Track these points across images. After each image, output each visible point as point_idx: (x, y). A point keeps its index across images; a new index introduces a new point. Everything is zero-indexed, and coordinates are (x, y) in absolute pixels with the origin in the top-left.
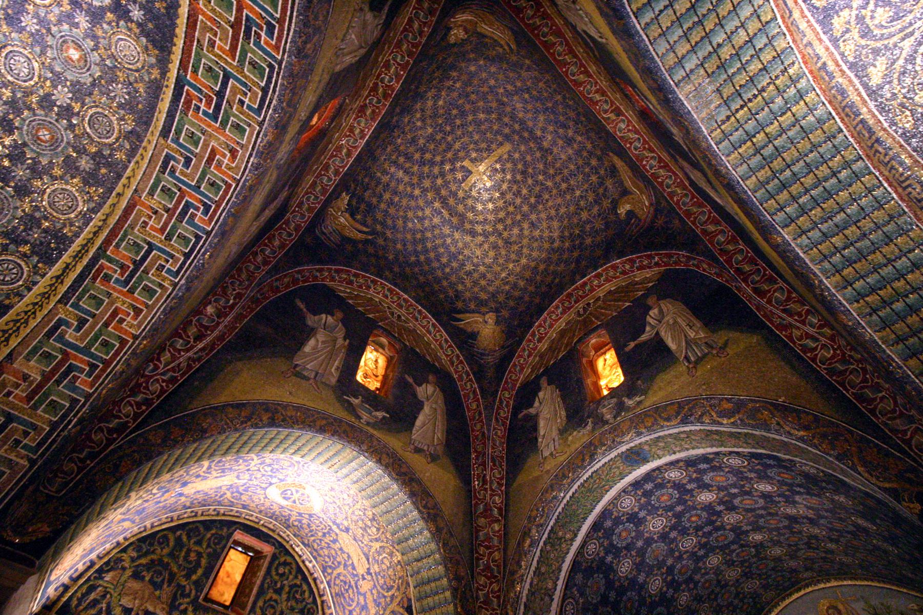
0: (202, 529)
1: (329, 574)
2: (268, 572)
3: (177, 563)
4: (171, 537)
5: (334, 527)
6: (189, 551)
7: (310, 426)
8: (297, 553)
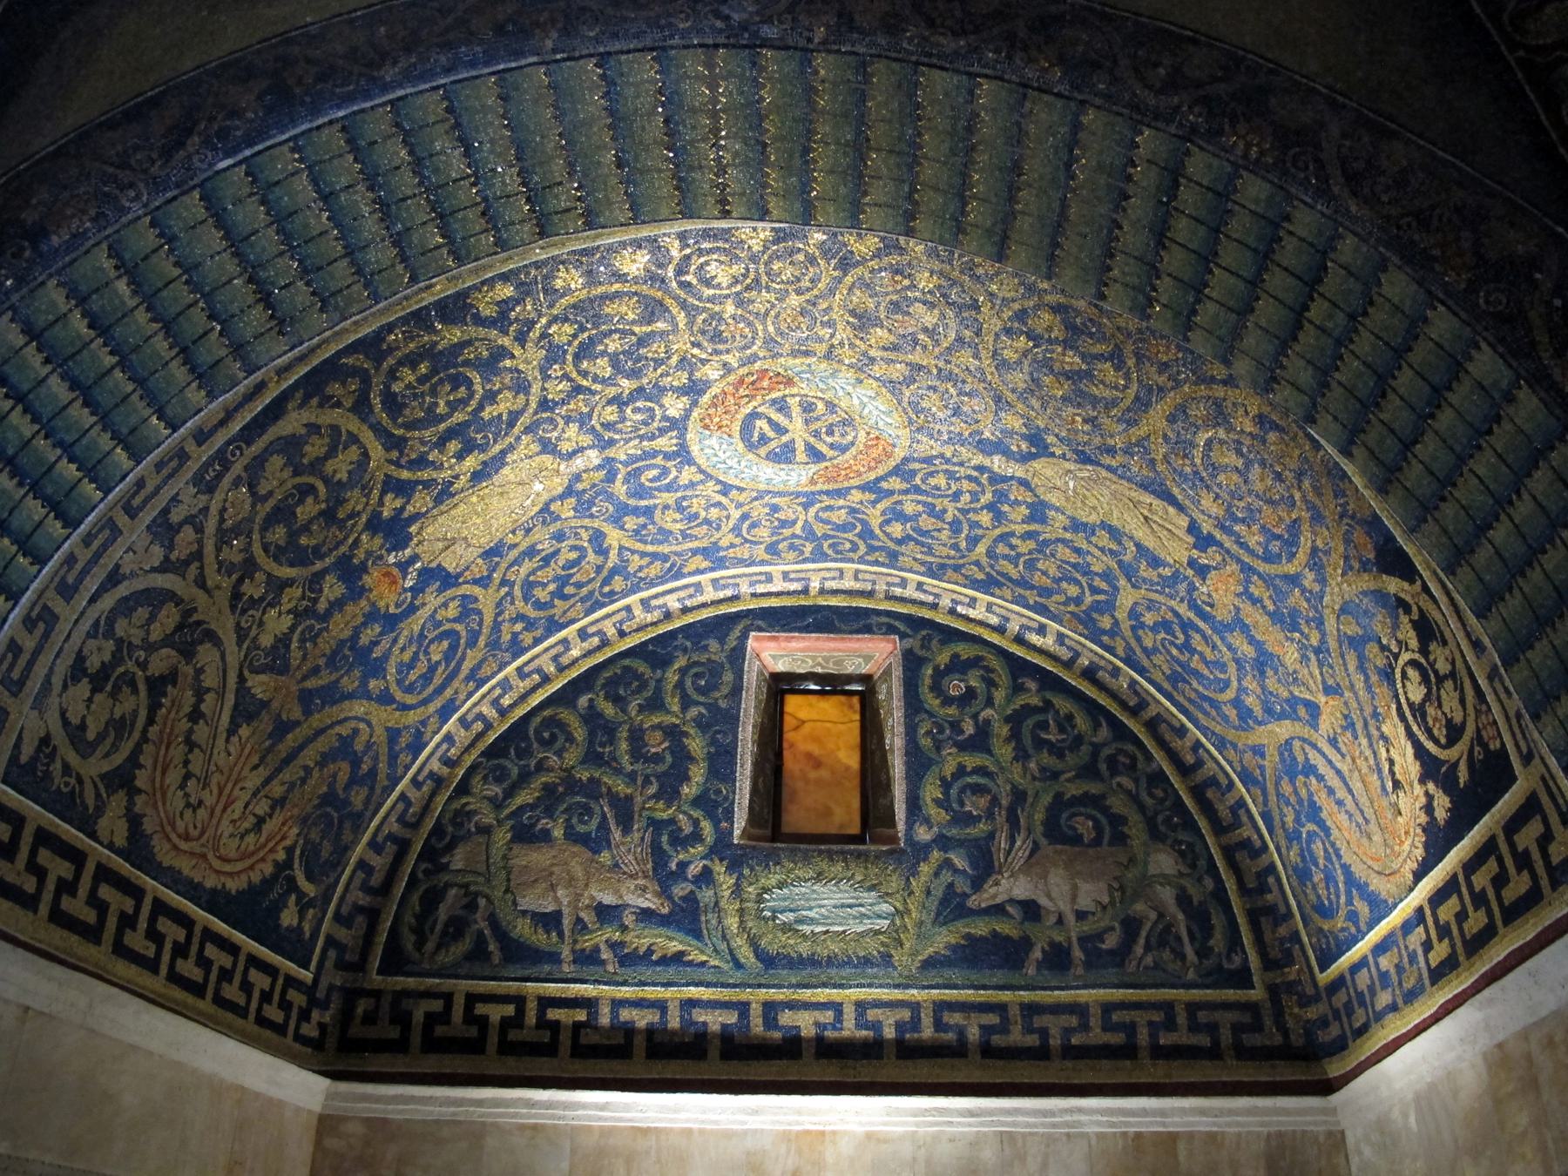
0: (642, 667)
1: (1114, 632)
2: (913, 704)
3: (618, 771)
4: (565, 715)
5: (997, 463)
6: (637, 737)
7: (447, 46)
8: (981, 623)
